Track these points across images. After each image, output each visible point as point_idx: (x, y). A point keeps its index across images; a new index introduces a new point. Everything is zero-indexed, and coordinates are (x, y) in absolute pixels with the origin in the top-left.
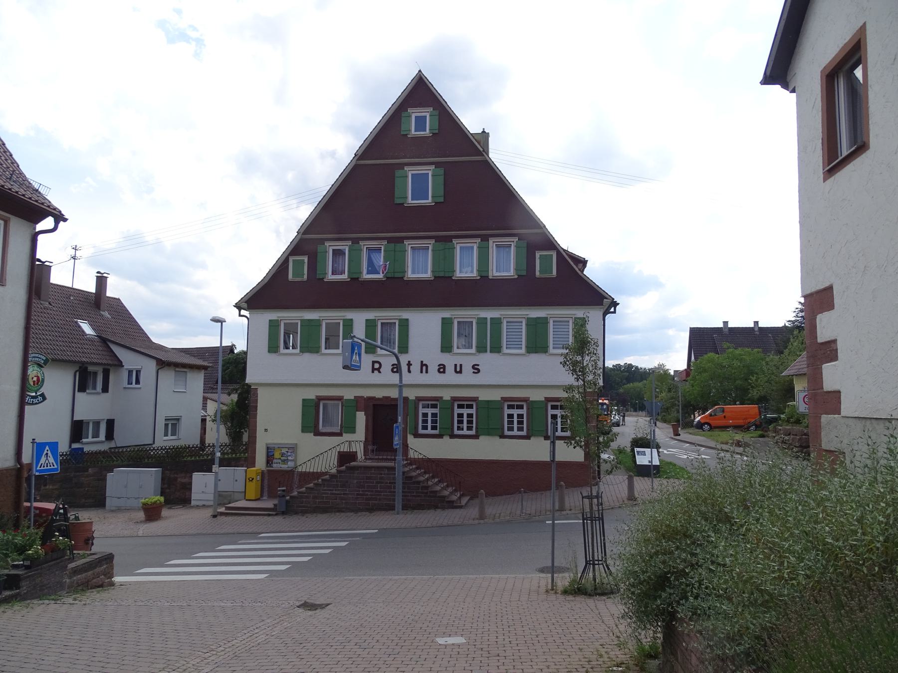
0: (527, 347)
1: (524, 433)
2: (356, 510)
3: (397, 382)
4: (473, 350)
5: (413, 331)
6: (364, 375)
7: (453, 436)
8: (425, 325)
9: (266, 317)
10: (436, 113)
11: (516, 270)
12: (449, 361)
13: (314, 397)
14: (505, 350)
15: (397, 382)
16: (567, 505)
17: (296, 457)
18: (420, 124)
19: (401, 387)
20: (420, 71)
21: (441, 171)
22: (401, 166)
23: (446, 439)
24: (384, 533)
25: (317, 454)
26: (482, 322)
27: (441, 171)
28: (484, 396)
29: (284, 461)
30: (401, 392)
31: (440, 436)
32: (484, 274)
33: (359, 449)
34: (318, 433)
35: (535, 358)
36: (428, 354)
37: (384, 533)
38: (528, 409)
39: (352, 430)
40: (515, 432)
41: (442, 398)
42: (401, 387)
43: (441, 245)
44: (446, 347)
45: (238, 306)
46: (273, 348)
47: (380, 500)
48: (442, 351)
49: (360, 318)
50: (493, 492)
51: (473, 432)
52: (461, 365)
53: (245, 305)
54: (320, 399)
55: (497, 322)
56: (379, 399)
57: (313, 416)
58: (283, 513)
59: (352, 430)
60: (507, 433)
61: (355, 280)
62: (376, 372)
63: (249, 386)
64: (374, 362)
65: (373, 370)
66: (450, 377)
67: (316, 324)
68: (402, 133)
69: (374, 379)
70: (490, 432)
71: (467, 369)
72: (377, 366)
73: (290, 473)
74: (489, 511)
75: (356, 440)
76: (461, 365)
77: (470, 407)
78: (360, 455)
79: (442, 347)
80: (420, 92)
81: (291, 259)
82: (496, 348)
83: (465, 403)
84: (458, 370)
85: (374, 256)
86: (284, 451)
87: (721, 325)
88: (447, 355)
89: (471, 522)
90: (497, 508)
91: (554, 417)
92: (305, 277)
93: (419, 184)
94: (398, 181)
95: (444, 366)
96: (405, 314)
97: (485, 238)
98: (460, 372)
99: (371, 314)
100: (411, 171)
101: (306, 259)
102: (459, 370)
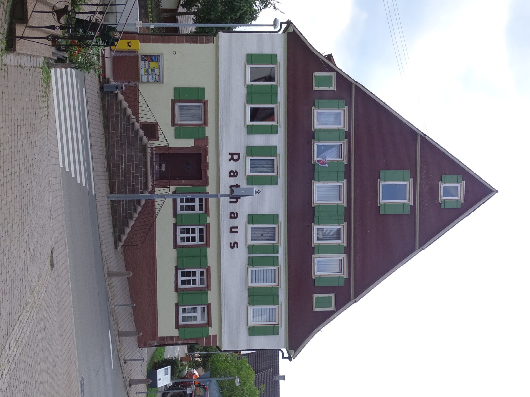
0: (253, 288)
1: (180, 286)
2: (108, 157)
3: (221, 193)
4: (250, 242)
5: (265, 189)
6: (226, 166)
7: (175, 226)
8: (272, 200)
9: (278, 47)
10: (459, 206)
11: (320, 278)
12: (241, 222)
13: (206, 99)
14: (250, 269)
15: (221, 193)
16: (114, 279)
17: (152, 83)
18: (451, 192)
19: (217, 196)
20: (497, 191)
21: (407, 211)
22: (413, 176)
23: (173, 220)
24: (93, 199)
25: (155, 103)
26: (275, 249)
27: (407, 211)
28: (211, 252)
29: (147, 71)
30: (213, 196)
31: (175, 215)
32: (316, 250)
33: (160, 143)
34: (173, 102)
35: (244, 295)
36: (246, 204)
37: (93, 199)
38: (200, 289)
39: (178, 135)
40: (179, 235)
41: (209, 215)
42: (217, 196)
43: (342, 212)
44: (252, 219)
45: (289, 23)
46: (251, 58)
47: (118, 176)
48: (249, 215)
49: (278, 140)
50: (131, 282)
51: (179, 243)
52: (237, 232)
53: (291, 30)
54: (205, 103)
55: (274, 261)
56: (206, 159)
57: (190, 98)
58: (102, 88)
59: (178, 135)
60: (180, 272)
61: (312, 136)
62: (230, 157)
63: (216, 34)
64: (238, 154)
65: (232, 154)
66: (226, 223)
67: (274, 101)
68: (443, 176)
69: (222, 171)
70: (180, 257)
71: (234, 238)
72: (235, 157)
73: (136, 78)
74: (115, 280)
75: (168, 138)
76: (237, 232)
77: (201, 239)
78: (155, 143)
79: (253, 215)
80: (478, 191)
81: (333, 74)
82: (252, 262)
83: (204, 235)
84: (233, 230)
85: (335, 151)
86: (157, 71)
87: (281, 374)
88: (245, 219)
89: (106, 268)
90: (114, 260)
91: (194, 274)
92: (316, 89)
93: (396, 192)
94: (400, 173)
95: (236, 217)
96: (282, 181)
97: (347, 250)
98: (231, 232)
99: (281, 151)
100: (408, 184)
101: (333, 88)
102: (233, 230)
